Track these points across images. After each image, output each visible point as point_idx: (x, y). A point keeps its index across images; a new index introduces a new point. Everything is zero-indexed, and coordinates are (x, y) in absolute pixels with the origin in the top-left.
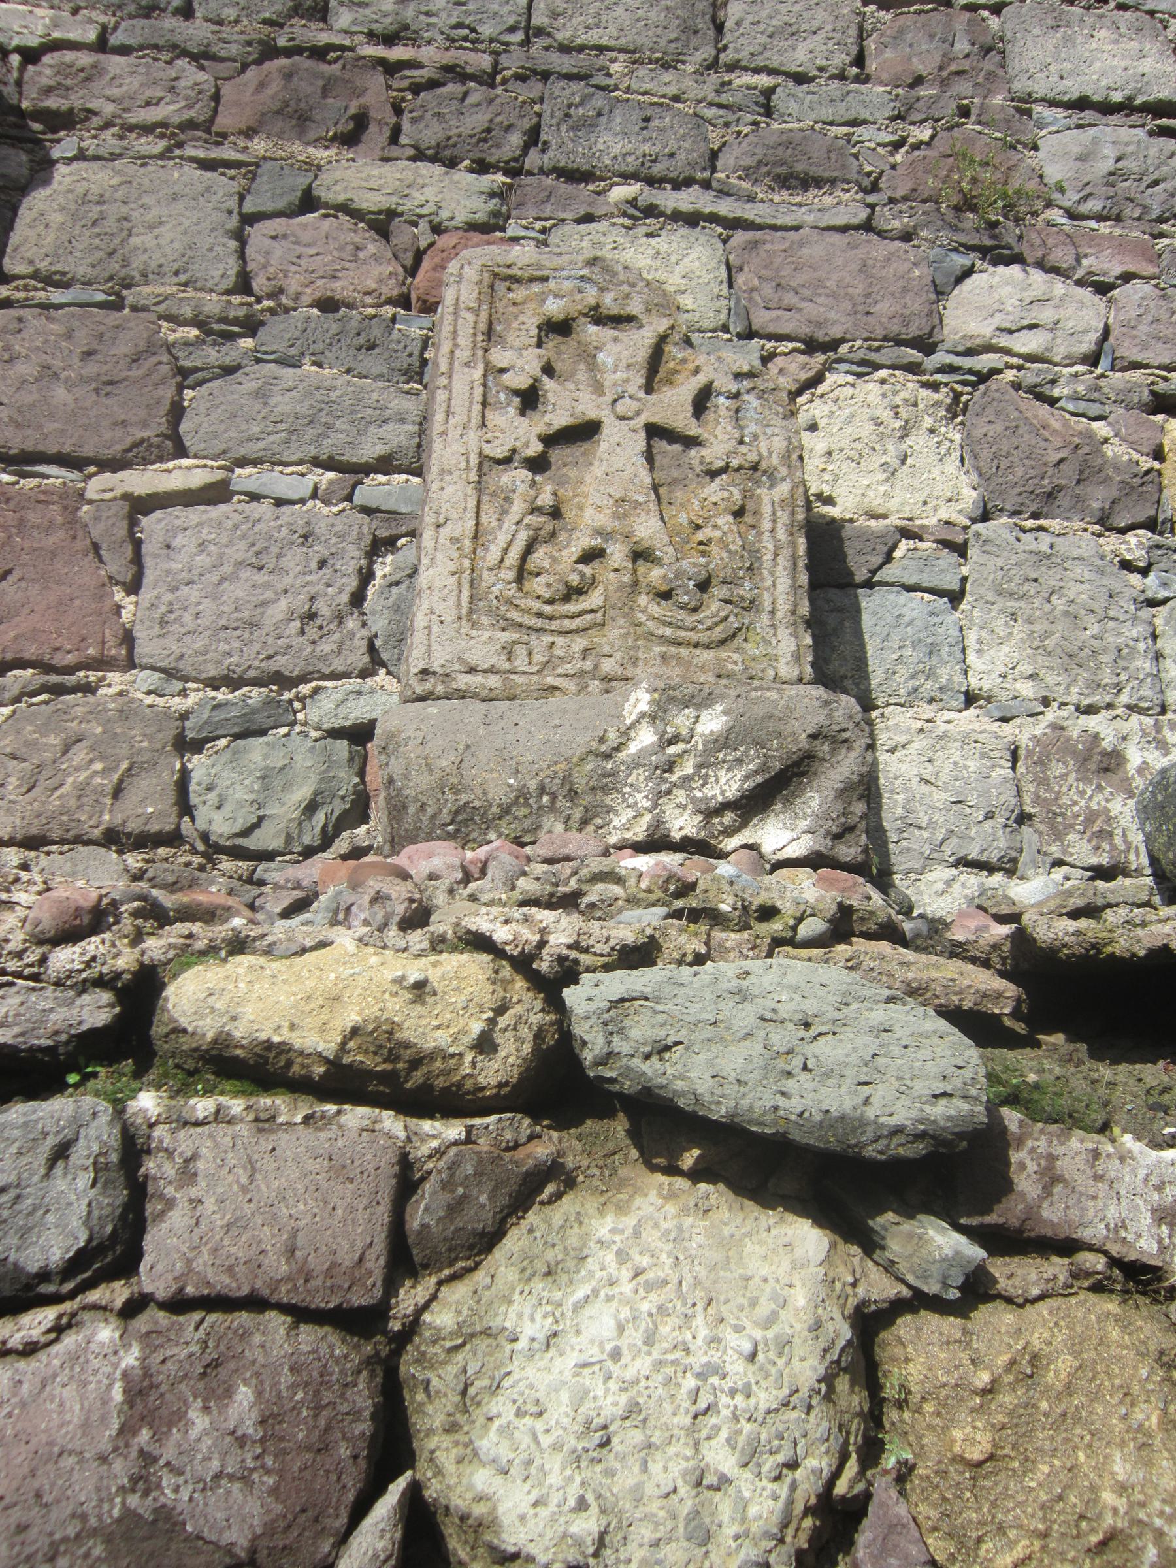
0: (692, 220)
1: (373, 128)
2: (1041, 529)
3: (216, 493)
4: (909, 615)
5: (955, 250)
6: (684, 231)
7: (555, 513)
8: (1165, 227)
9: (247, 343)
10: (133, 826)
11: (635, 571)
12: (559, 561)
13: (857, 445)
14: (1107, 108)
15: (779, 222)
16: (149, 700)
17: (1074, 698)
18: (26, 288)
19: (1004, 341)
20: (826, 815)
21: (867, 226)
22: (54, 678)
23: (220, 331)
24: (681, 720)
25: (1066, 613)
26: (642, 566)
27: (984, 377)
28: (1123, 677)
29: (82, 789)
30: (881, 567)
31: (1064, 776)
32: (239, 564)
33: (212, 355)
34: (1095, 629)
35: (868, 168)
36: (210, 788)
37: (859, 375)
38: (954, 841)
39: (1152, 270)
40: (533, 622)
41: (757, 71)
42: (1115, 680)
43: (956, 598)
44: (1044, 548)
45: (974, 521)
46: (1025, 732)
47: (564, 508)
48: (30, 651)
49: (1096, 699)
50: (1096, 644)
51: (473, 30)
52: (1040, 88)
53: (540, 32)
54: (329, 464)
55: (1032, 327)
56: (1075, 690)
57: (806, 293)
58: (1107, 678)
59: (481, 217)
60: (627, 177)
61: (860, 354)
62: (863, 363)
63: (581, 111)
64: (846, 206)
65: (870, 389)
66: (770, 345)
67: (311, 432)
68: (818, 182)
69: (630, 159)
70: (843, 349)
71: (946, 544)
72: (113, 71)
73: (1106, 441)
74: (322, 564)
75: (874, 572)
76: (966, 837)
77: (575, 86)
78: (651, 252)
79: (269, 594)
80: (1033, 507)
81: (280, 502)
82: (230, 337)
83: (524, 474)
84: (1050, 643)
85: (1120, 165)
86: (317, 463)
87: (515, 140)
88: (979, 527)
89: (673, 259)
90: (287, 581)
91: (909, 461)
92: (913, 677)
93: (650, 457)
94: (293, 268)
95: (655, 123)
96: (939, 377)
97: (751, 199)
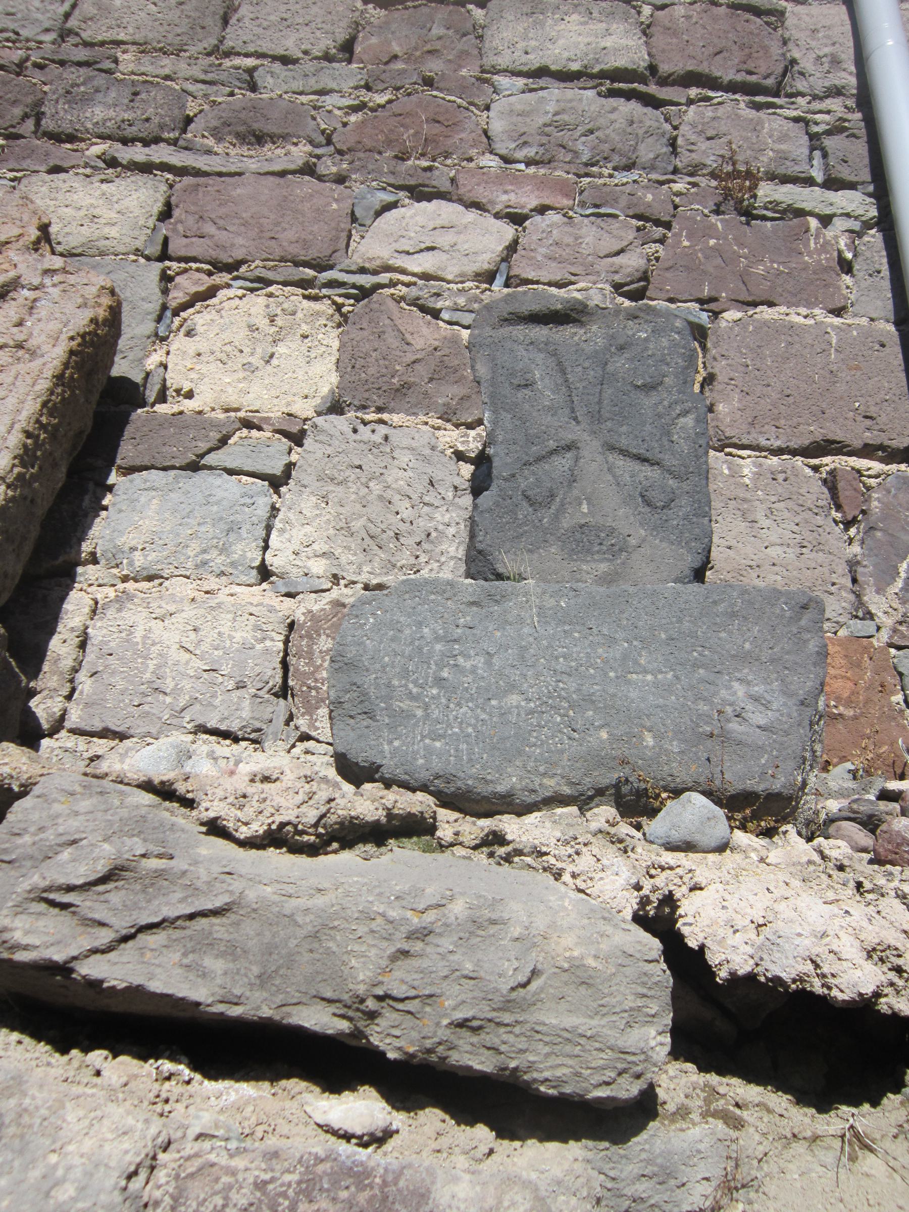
0: (146, 168)
2: (381, 422)
5: (384, 189)
8: (594, 169)
13: (228, 348)
14: (566, 77)
15: (224, 170)
17: (364, 578)
25: (380, 497)
27: (364, 293)
30: (210, 451)
35: (323, 126)
37: (252, 290)
38: (197, 707)
39: (566, 202)
41: (247, 55)
42: (412, 561)
43: (276, 482)
45: (319, 414)
51: (17, 34)
52: (503, 61)
53: (70, 32)
55: (432, 249)
56: (366, 569)
60: (103, 137)
61: (257, 273)
62: (259, 280)
63: (82, 89)
65: (257, 303)
68: (273, 138)
69: (108, 124)
70: (243, 269)
75: (202, 456)
76: (210, 704)
77: (83, 71)
85: (557, 118)
89: (115, 199)
91: (275, 362)
92: (204, 551)
95: (143, 96)
96: (325, 291)
97: (209, 152)
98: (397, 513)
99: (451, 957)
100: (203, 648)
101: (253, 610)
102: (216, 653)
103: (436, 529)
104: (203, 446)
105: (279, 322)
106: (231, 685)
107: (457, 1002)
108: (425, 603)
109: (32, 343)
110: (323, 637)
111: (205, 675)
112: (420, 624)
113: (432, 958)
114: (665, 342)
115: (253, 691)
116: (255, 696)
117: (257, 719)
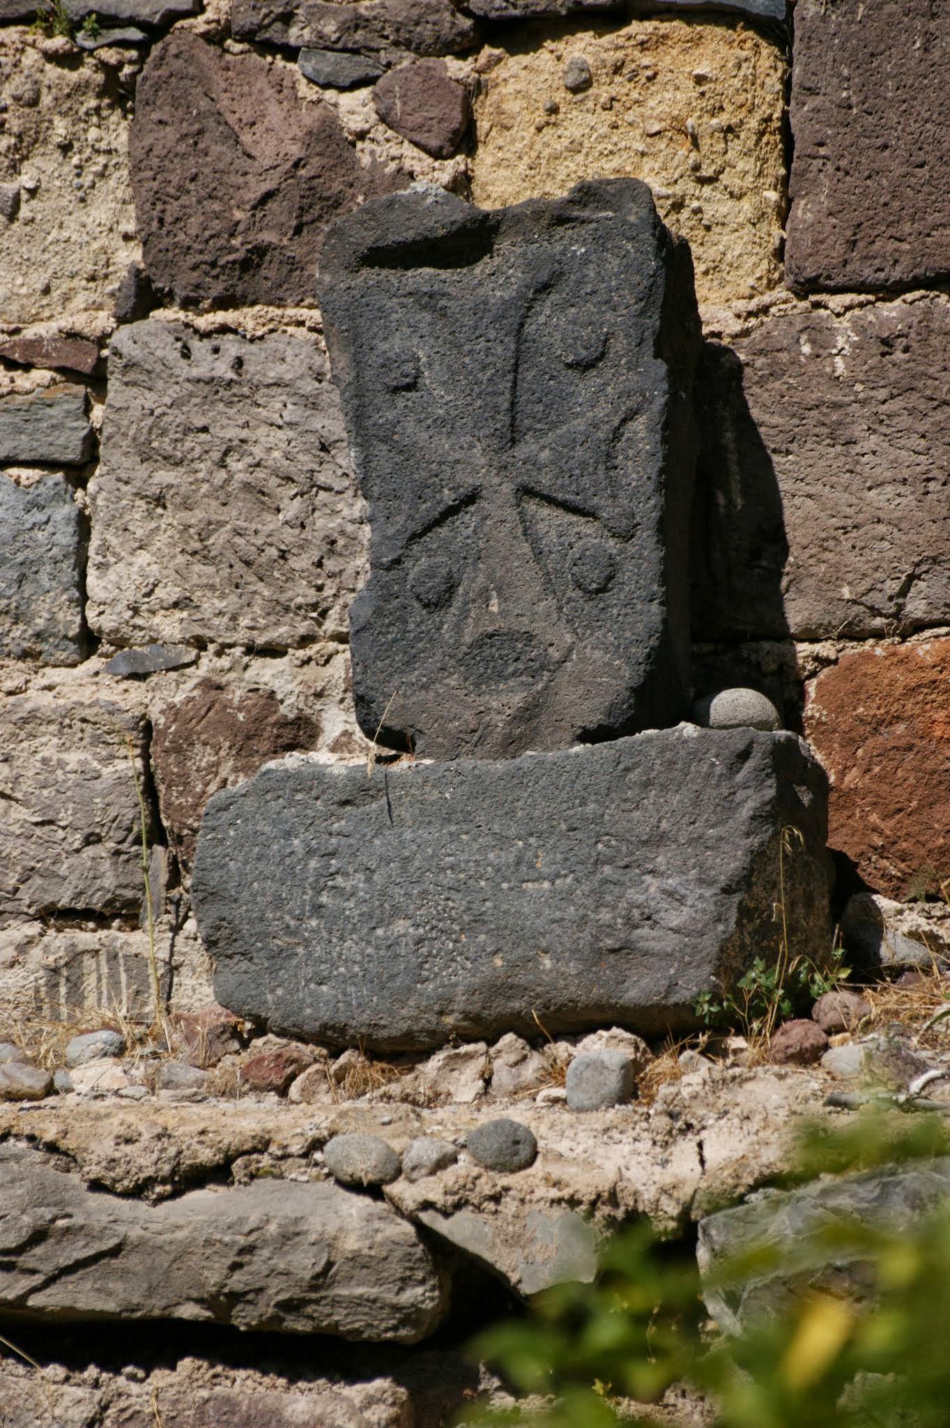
17: (241, 636)
28: (328, 592)
31: (214, 768)
34: (292, 509)
38: (37, 881)
42: (312, 595)
43: (78, 472)
44: (223, 369)
46: (161, 697)
50: (289, 535)
56: (244, 622)
58: (302, 593)
71: (69, 374)
73: (362, 135)
76: (54, 875)
80: (217, 289)
84: (218, 540)
88: (122, 337)
98: (278, 510)
99: (271, 1262)
100: (24, 788)
101: (88, 713)
102: (45, 792)
103: (342, 533)
106: (77, 840)
107: (278, 1291)
108: (290, 806)
110: (198, 747)
111: (38, 831)
112: (288, 835)
113: (259, 1262)
114: (614, 264)
115: (111, 845)
116: (117, 853)
117: (126, 887)
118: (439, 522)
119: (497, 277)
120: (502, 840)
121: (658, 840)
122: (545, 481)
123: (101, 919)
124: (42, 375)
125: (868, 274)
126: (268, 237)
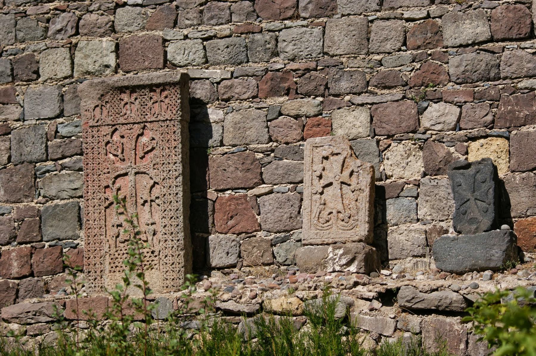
0: (362, 105)
1: (291, 90)
3: (271, 192)
4: (405, 203)
6: (360, 108)
7: (325, 204)
9: (272, 155)
10: (266, 262)
11: (338, 216)
12: (325, 214)
14: (467, 45)
15: (382, 101)
16: (265, 238)
17: (438, 219)
18: (229, 149)
19: (433, 128)
20: (357, 265)
21: (404, 97)
22: (249, 235)
23: (266, 153)
24: (337, 251)
26: (339, 214)
27: (426, 140)
29: (256, 256)
31: (435, 237)
32: (277, 208)
33: (266, 160)
34: (445, 202)
36: (278, 253)
40: (321, 228)
43: (416, 198)
44: (435, 184)
46: (428, 227)
47: (326, 202)
48: (244, 231)
49: (444, 218)
54: (291, 183)
57: (387, 123)
58: (446, 213)
59: (316, 113)
60: (348, 94)
63: (337, 76)
64: (397, 93)
66: (379, 137)
67: (286, 176)
69: (348, 89)
71: (415, 185)
72: (235, 84)
74: (292, 206)
78: (353, 117)
79: (283, 214)
80: (434, 173)
81: (283, 193)
82: (268, 155)
83: (319, 196)
84: (435, 206)
85: (466, 68)
86: (288, 183)
87: (322, 88)
88: (422, 180)
90: (286, 210)
93: (341, 189)
94: (279, 135)
104: (399, 191)
105: (408, 153)
106: (417, 246)
107: (445, 305)
109: (362, 188)
113: (442, 301)
114: (487, 169)
118: (464, 203)
119: (471, 171)
120: (473, 245)
121: (494, 245)
122: (478, 198)
123: (420, 257)
124: (411, 185)
125: (521, 170)
126: (441, 166)
